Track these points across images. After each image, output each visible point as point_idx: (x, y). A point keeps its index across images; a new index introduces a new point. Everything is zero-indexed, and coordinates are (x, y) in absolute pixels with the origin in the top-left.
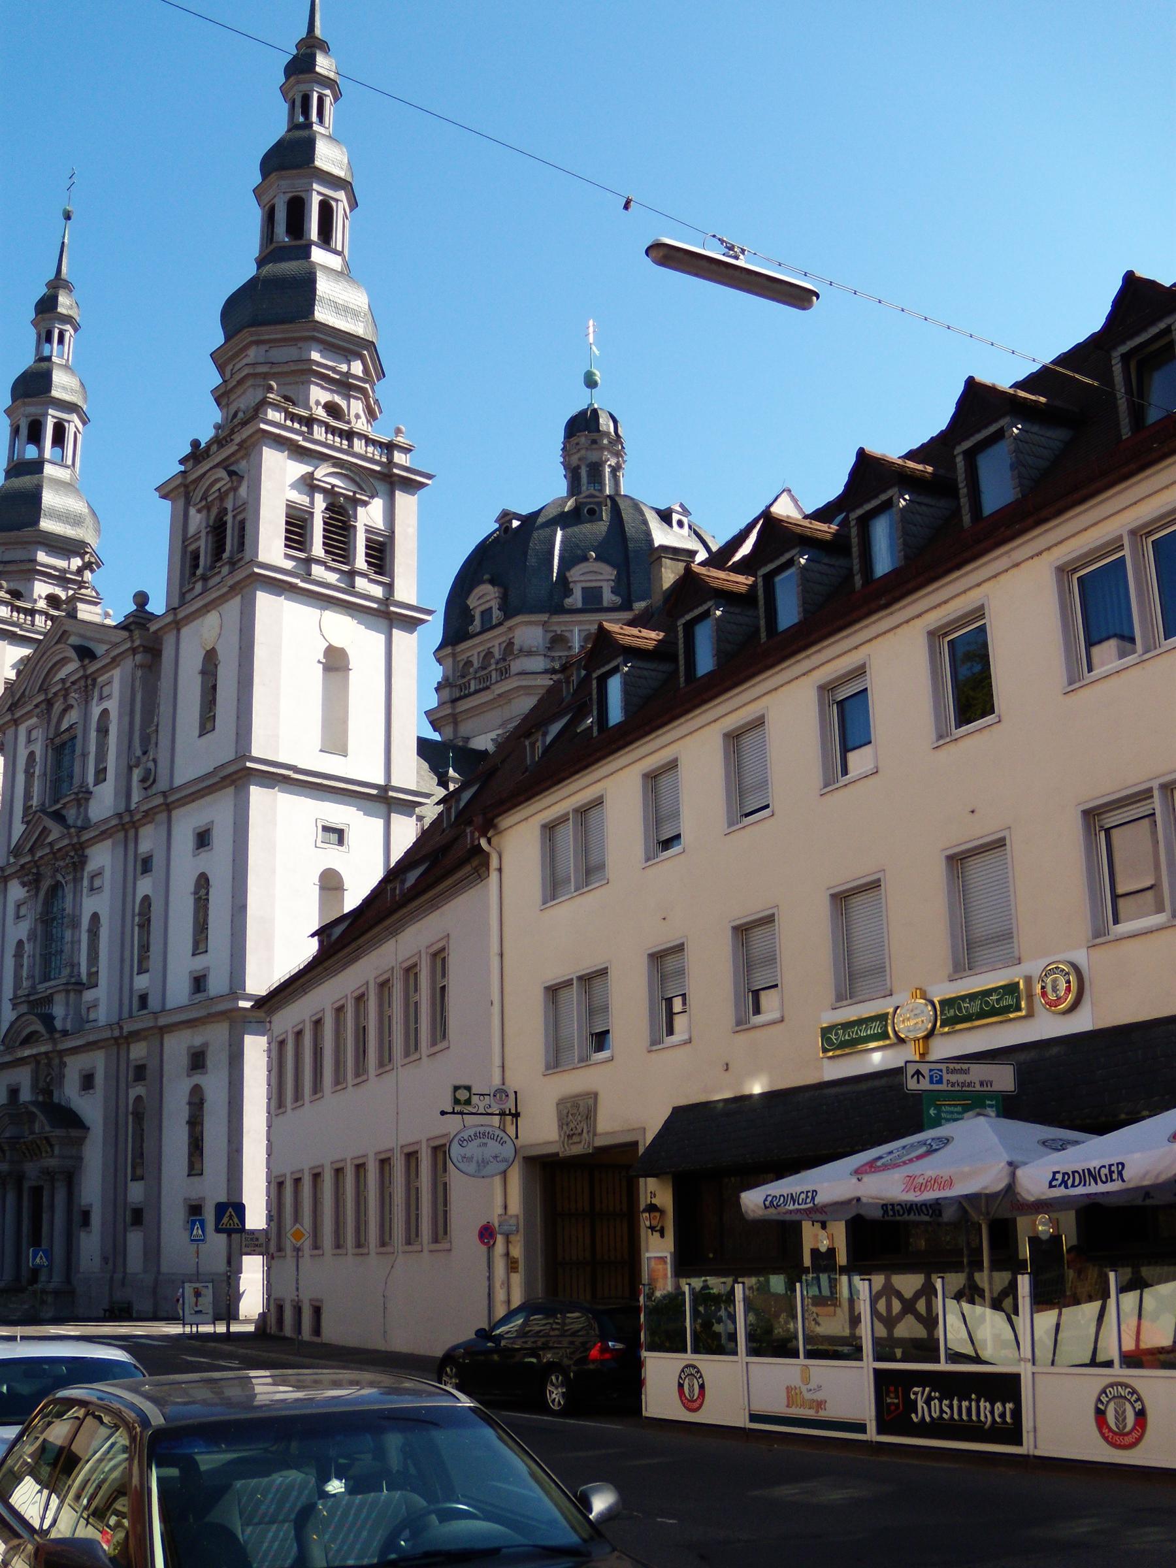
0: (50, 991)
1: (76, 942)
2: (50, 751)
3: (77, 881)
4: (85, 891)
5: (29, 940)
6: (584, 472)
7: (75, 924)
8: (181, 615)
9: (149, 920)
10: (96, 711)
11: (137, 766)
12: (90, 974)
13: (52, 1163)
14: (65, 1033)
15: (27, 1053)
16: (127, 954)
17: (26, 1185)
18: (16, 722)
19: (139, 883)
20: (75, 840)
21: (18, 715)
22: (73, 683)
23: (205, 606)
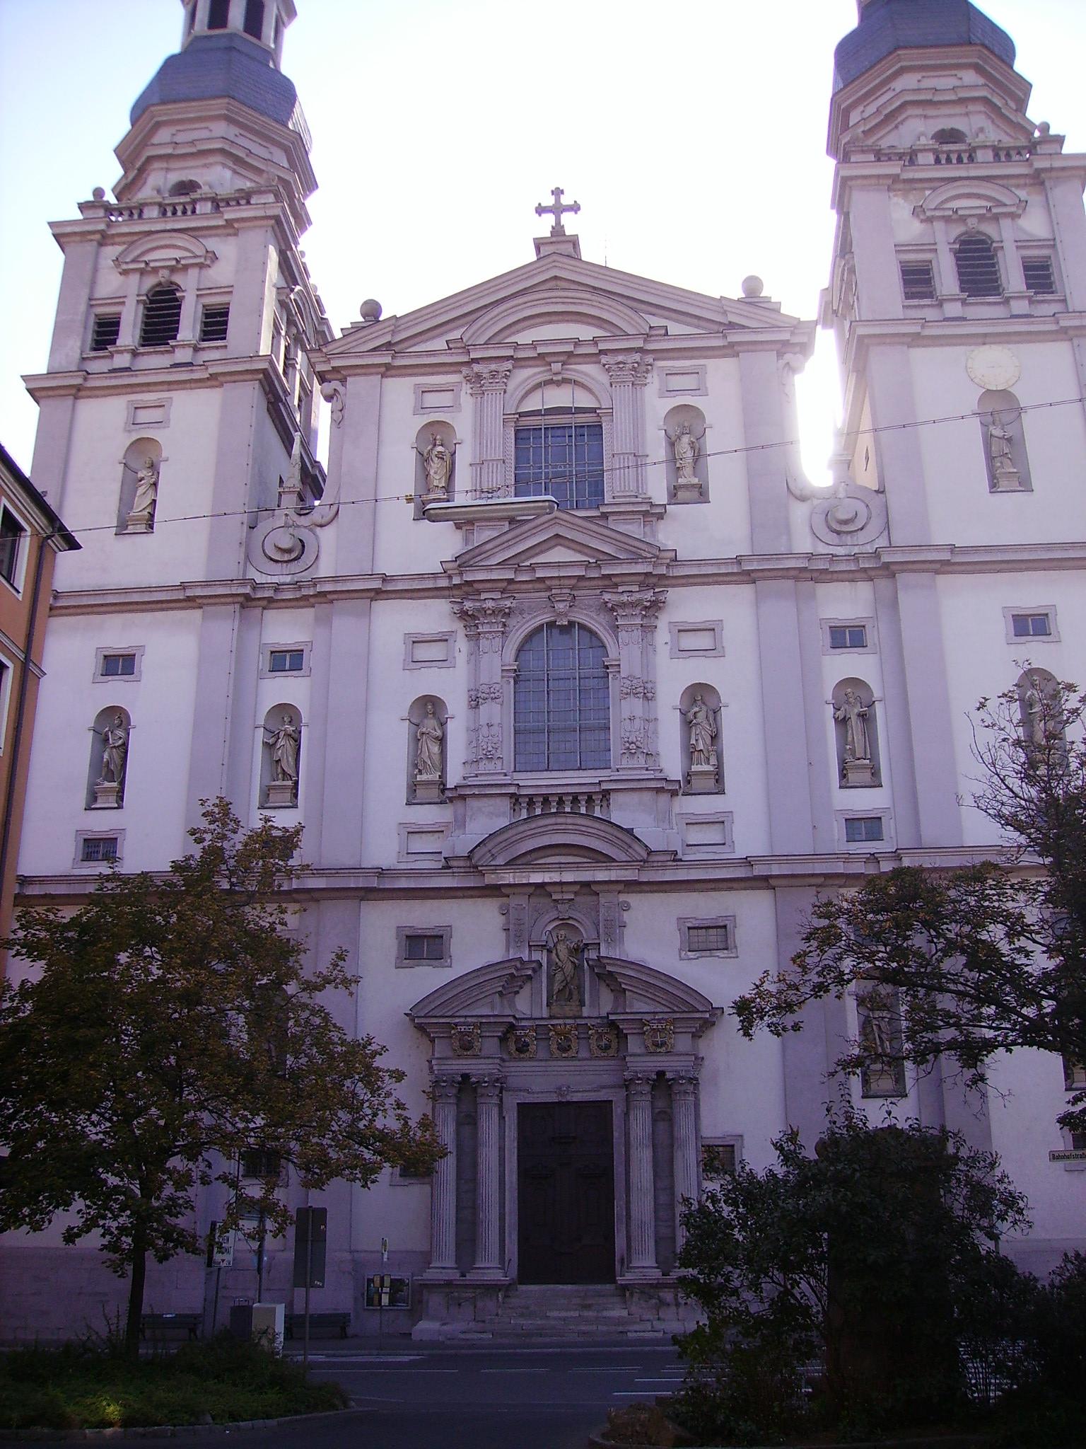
0: (604, 786)
5: (475, 702)
7: (648, 695)
8: (927, 332)
9: (866, 718)
10: (656, 404)
12: (688, 777)
13: (670, 1065)
14: (674, 857)
15: (537, 878)
17: (511, 1101)
18: (388, 371)
21: (398, 362)
22: (602, 352)
23: (985, 335)
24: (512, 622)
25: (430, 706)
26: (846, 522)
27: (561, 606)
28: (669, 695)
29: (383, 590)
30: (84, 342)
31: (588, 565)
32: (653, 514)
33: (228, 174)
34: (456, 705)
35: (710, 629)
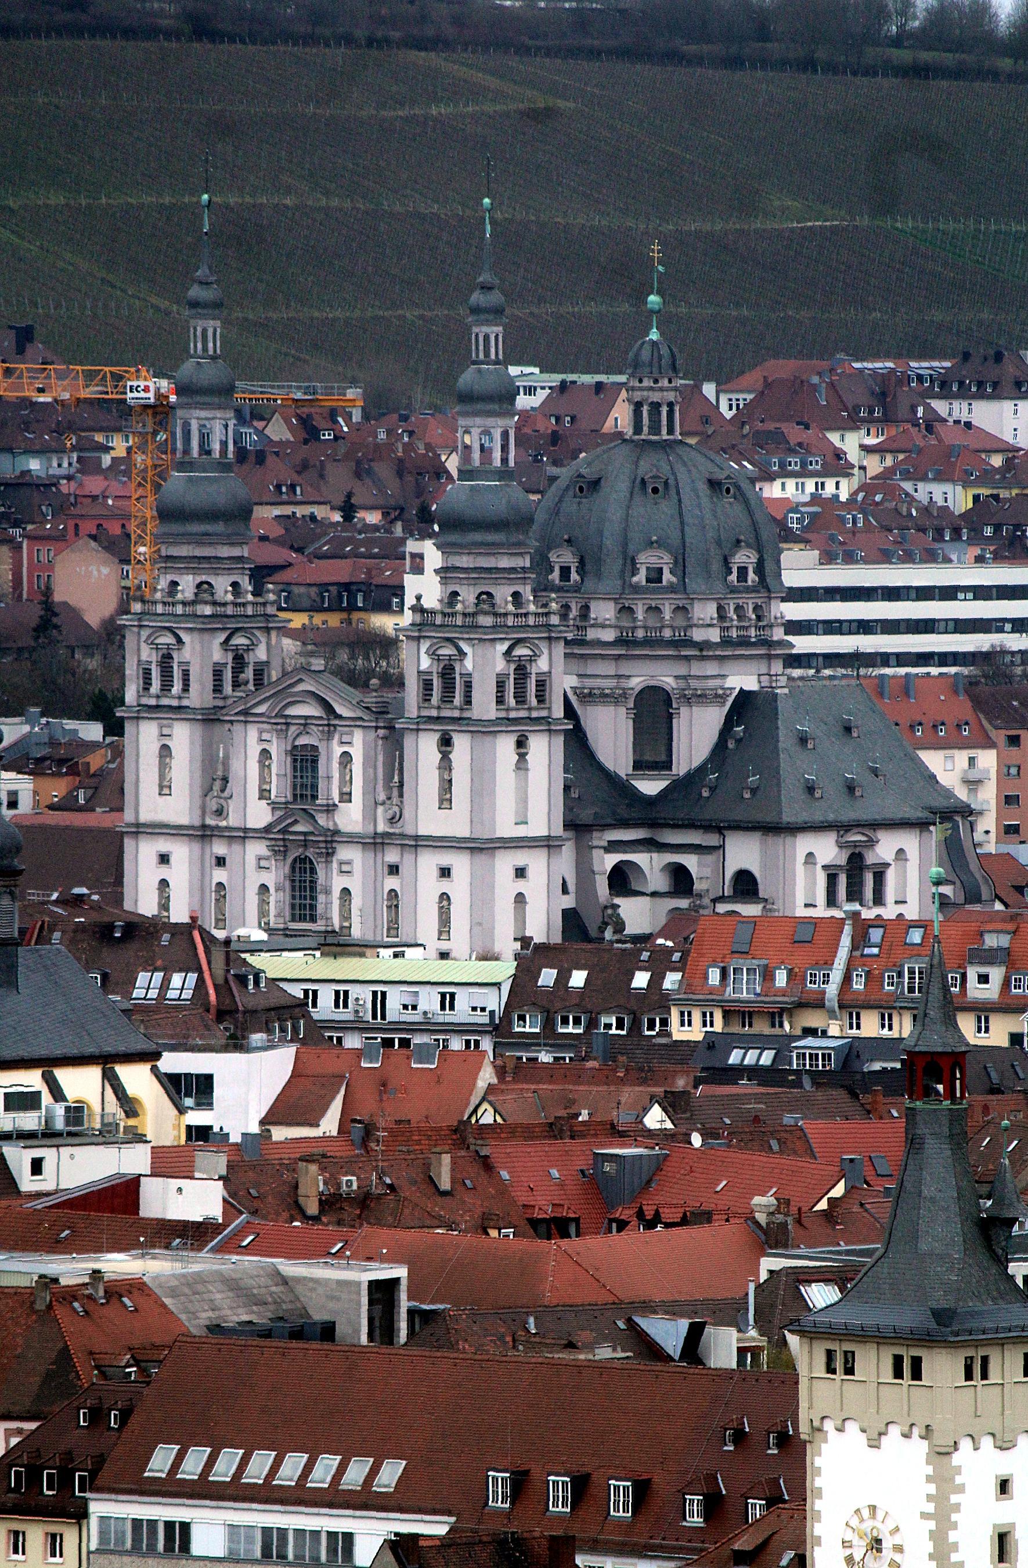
1: (328, 904)
2: (289, 759)
3: (328, 862)
4: (335, 872)
6: (645, 409)
7: (328, 892)
9: (397, 906)
11: (381, 804)
12: (342, 928)
16: (379, 922)
19: (386, 880)
20: (329, 839)
24: (289, 854)
25: (264, 888)
26: (393, 818)
27: (300, 850)
28: (336, 893)
29: (244, 835)
30: (138, 685)
31: (305, 834)
32: (330, 809)
33: (191, 577)
34: (272, 890)
35: (349, 863)
